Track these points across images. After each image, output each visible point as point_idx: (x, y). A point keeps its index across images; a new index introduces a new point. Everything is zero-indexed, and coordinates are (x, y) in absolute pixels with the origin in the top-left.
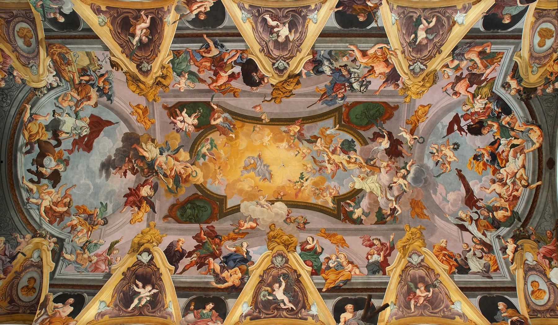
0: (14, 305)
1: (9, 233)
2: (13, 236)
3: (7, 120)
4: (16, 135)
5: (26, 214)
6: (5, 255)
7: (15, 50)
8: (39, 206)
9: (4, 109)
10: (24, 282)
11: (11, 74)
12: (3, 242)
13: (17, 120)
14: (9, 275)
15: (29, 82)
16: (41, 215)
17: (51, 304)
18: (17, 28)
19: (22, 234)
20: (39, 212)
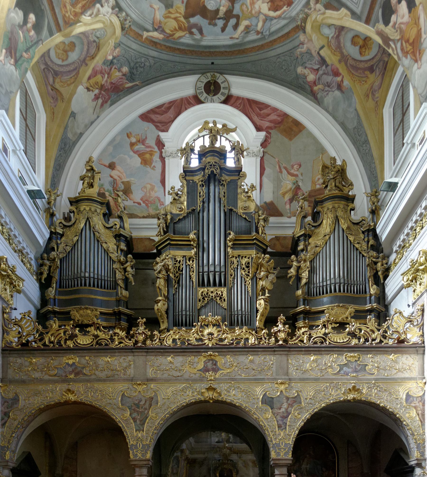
0: (376, 66)
1: (294, 62)
2: (299, 57)
3: (164, 60)
4: (182, 47)
5: (275, 37)
6: (318, 70)
7: (84, 62)
8: (267, 19)
9: (153, 64)
11: (112, 62)
12: (303, 70)
13: (163, 47)
14: (341, 71)
15: (116, 38)
16: (279, 17)
18: (60, 62)
19: (298, 46)
20: (275, 18)
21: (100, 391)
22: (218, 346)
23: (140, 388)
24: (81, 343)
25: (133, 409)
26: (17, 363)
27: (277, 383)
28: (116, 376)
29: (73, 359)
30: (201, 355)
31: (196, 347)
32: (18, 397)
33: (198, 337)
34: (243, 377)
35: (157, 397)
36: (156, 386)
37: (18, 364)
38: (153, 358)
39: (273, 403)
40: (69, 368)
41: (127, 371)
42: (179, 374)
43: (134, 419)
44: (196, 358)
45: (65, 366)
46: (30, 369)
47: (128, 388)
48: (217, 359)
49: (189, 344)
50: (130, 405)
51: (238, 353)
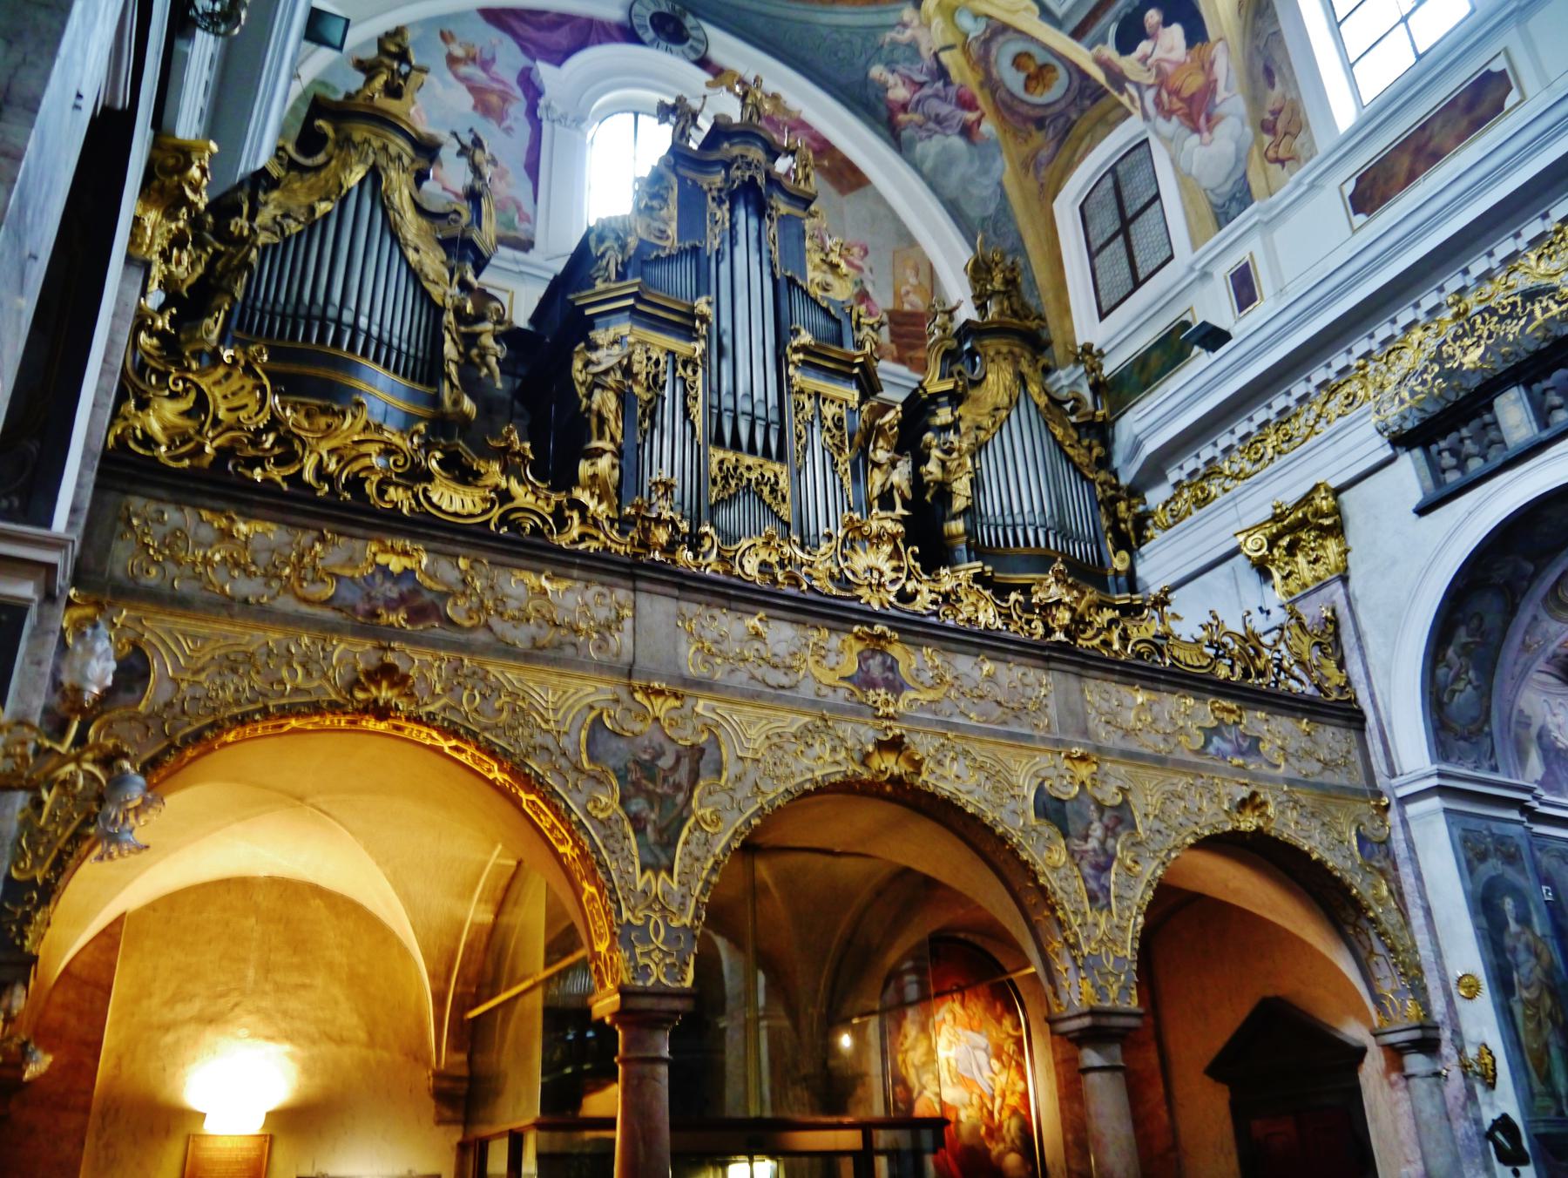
10: (1014, 80)
17: (1128, 64)
21: (510, 694)
22: (893, 612)
23: (661, 707)
24: (435, 499)
25: (633, 783)
26: (162, 523)
27: (1068, 757)
28: (569, 651)
29: (405, 553)
30: (850, 632)
31: (832, 601)
32: (146, 663)
33: (835, 570)
34: (973, 723)
35: (719, 748)
36: (714, 710)
37: (161, 530)
38: (700, 609)
39: (1065, 818)
40: (388, 585)
41: (611, 640)
42: (785, 681)
43: (638, 823)
44: (834, 636)
45: (373, 575)
46: (217, 557)
47: (617, 701)
48: (896, 650)
49: (811, 587)
50: (621, 765)
51: (953, 646)
